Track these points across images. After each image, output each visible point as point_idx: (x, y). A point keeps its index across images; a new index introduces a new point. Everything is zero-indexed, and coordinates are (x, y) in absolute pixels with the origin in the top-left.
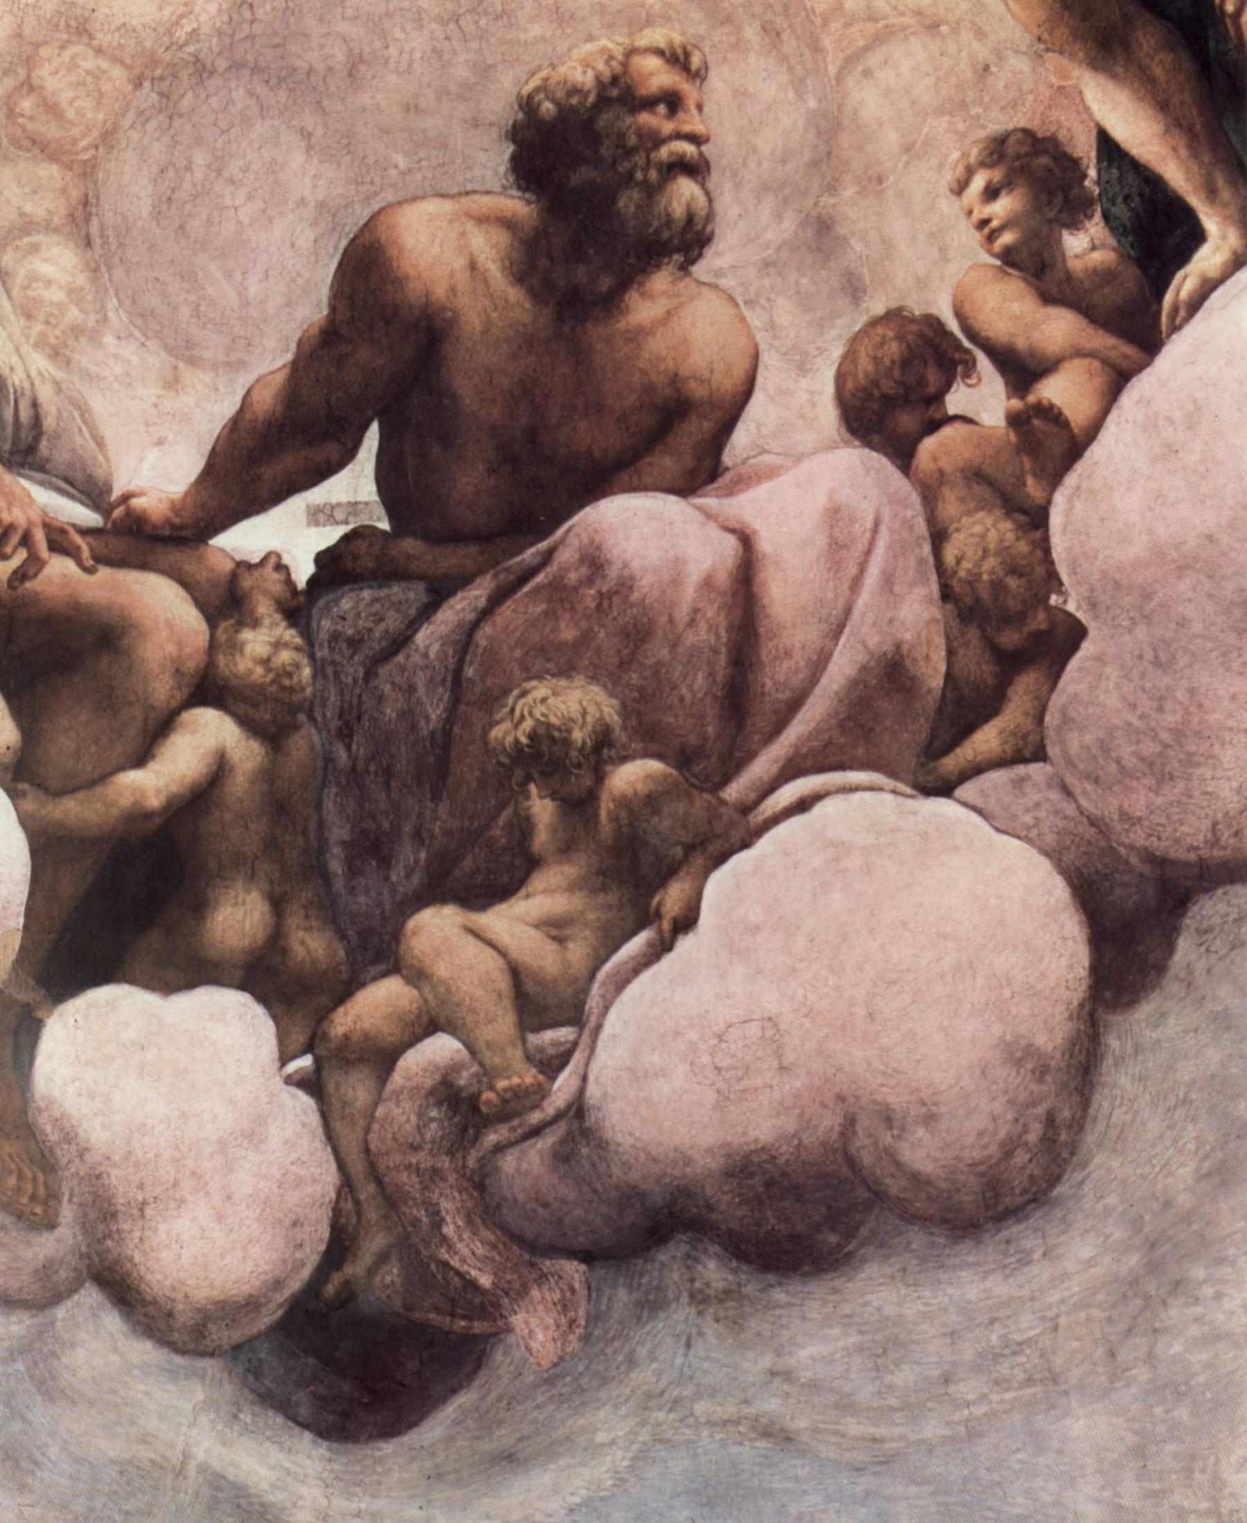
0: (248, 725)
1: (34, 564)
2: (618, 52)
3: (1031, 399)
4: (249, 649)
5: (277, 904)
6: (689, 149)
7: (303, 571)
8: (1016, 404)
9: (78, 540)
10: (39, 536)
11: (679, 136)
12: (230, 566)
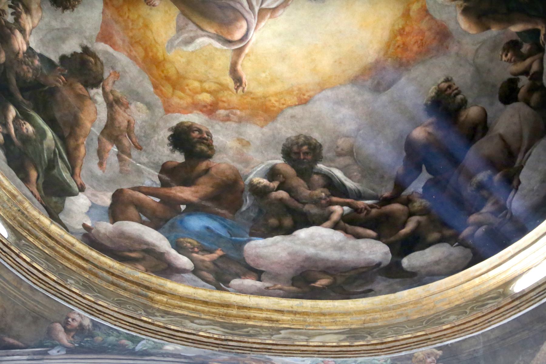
0: (420, 215)
1: (368, 212)
2: (437, 87)
3: (531, 74)
4: (416, 206)
5: (440, 232)
6: (456, 91)
7: (420, 190)
8: (529, 77)
9: (375, 205)
10: (368, 207)
11: (453, 91)
12: (406, 197)
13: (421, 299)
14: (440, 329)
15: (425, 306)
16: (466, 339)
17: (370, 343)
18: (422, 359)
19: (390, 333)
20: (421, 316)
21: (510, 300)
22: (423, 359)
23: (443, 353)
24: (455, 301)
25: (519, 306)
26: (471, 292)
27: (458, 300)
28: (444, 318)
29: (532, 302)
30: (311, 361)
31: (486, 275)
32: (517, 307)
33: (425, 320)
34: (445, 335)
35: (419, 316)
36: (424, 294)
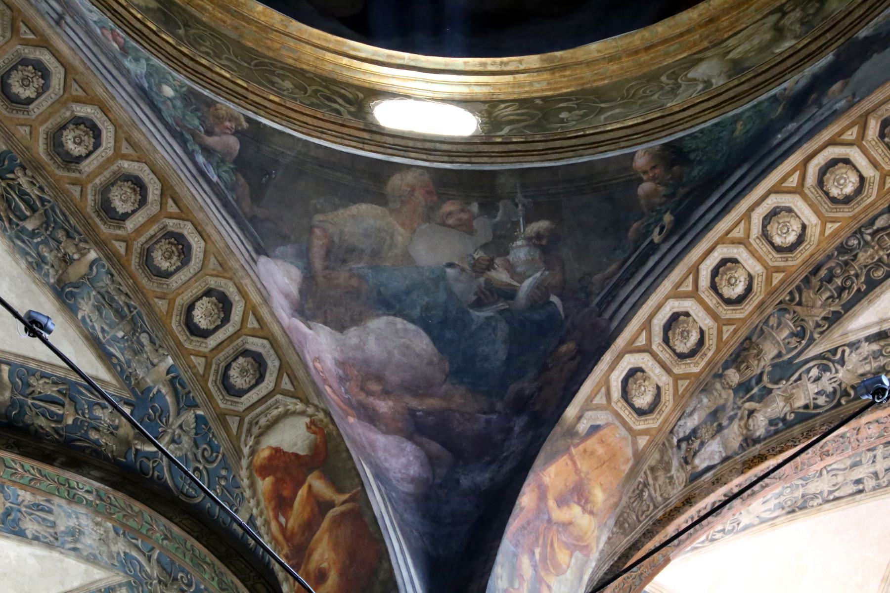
13: (271, 29)
14: (265, 96)
15: (268, 41)
16: (284, 133)
17: (179, 48)
18: (221, 116)
19: (208, 44)
20: (256, 49)
21: (362, 127)
22: (223, 118)
23: (248, 128)
24: (304, 63)
25: (366, 141)
26: (329, 67)
27: (308, 65)
28: (278, 77)
29: (382, 150)
30: (99, 18)
31: (359, 62)
32: (363, 141)
33: (257, 59)
34: (266, 107)
35: (254, 47)
36: (278, 26)
